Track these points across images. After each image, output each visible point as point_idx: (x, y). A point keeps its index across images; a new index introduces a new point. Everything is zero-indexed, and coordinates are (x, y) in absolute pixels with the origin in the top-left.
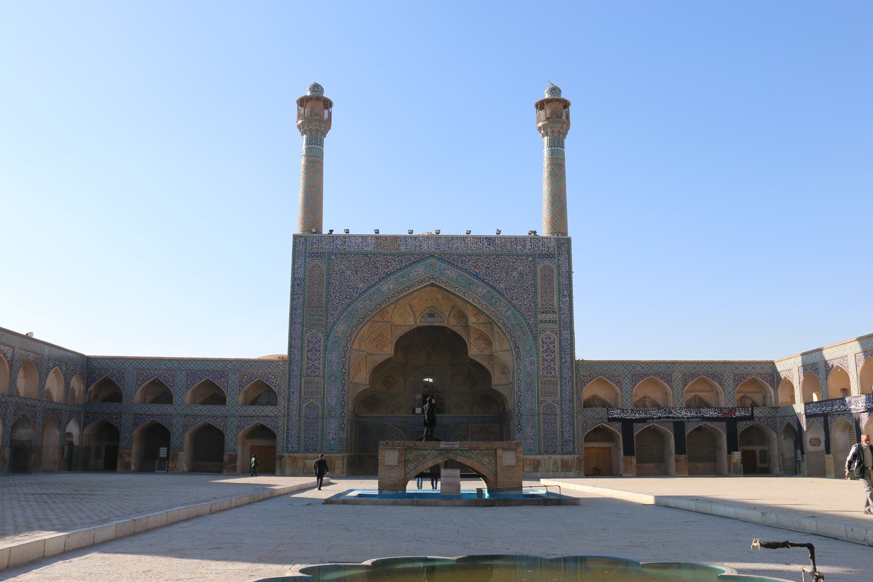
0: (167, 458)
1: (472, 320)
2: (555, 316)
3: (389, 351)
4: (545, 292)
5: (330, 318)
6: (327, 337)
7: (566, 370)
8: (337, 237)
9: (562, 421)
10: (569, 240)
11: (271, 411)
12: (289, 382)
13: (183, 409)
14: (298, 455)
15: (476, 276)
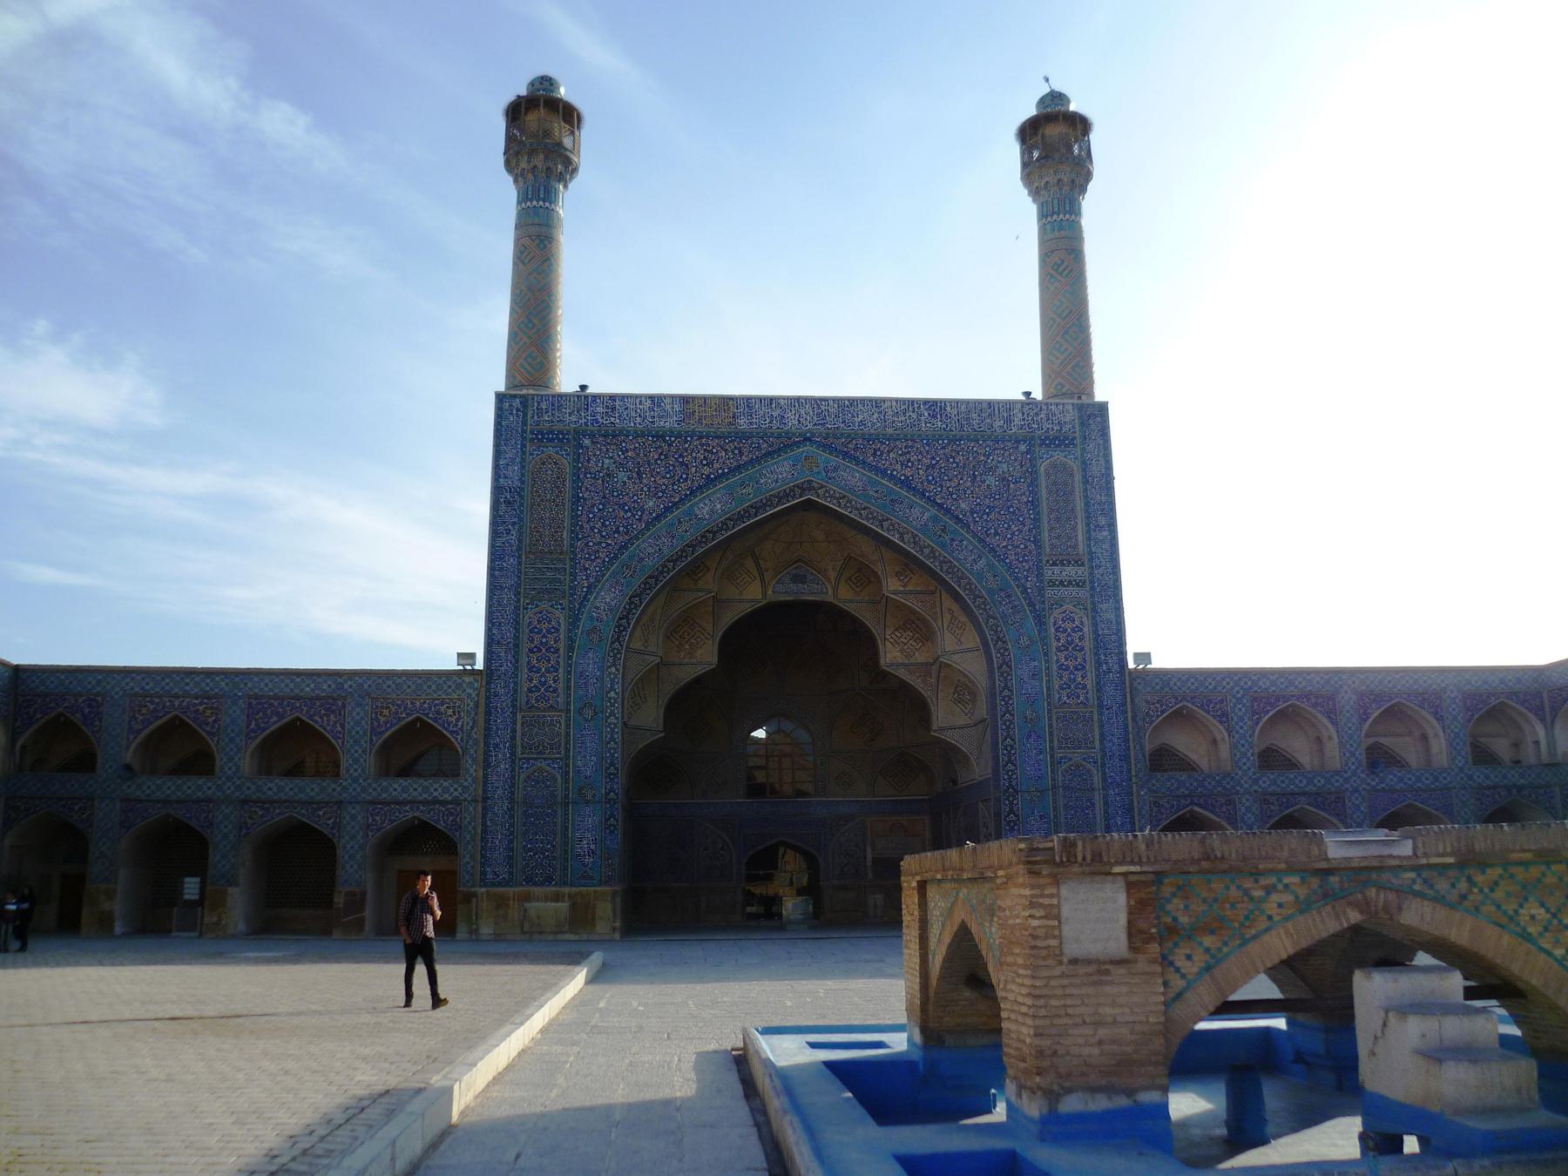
0: (200, 903)
1: (892, 585)
2: (1080, 570)
3: (705, 656)
4: (1058, 520)
5: (581, 576)
6: (574, 621)
7: (1109, 690)
8: (595, 397)
9: (1106, 803)
10: (1103, 408)
11: (446, 790)
12: (487, 721)
13: (238, 788)
14: (510, 890)
15: (906, 483)
